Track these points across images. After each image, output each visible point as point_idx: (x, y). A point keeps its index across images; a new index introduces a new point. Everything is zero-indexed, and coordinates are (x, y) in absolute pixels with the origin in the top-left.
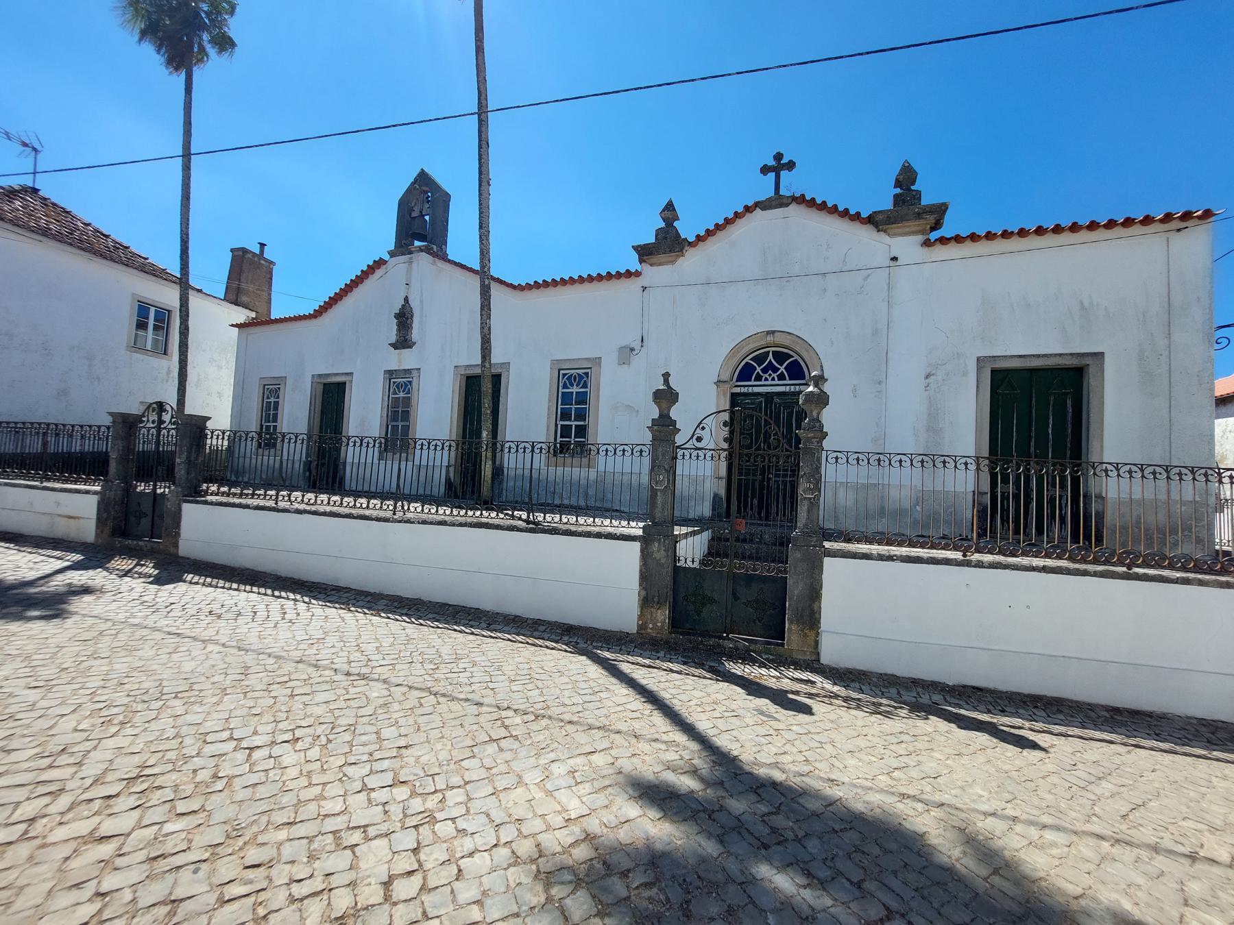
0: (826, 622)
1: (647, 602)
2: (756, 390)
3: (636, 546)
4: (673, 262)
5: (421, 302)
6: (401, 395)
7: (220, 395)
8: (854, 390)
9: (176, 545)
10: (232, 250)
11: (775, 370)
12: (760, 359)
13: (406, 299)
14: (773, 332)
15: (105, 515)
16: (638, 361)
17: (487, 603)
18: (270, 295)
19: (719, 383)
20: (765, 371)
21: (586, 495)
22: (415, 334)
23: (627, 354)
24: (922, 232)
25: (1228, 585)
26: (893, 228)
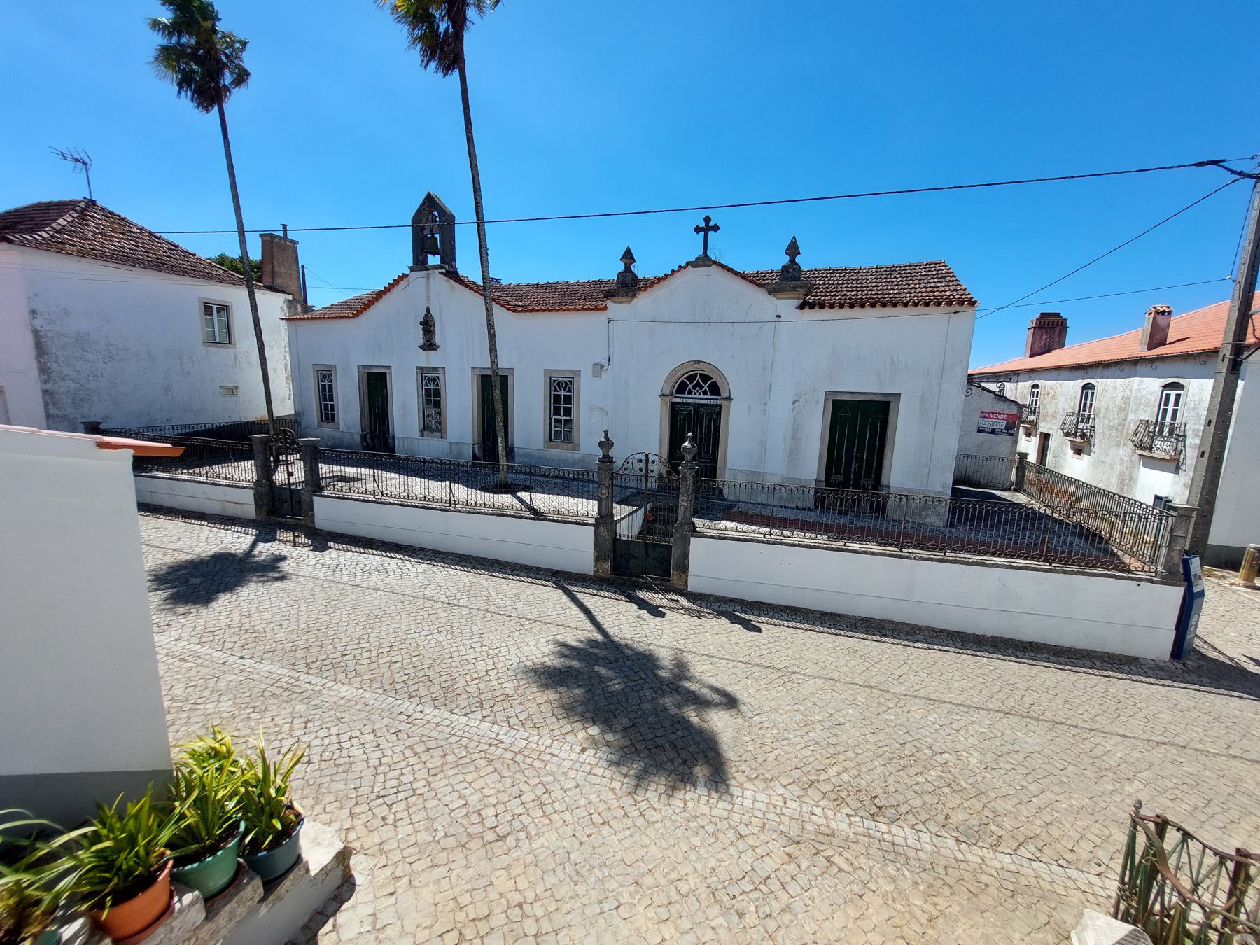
0: (691, 571)
4: (630, 302)
8: (749, 408)
9: (313, 522)
11: (701, 387)
12: (692, 378)
13: (428, 309)
14: (698, 362)
20: (694, 387)
22: (438, 339)
23: (599, 368)
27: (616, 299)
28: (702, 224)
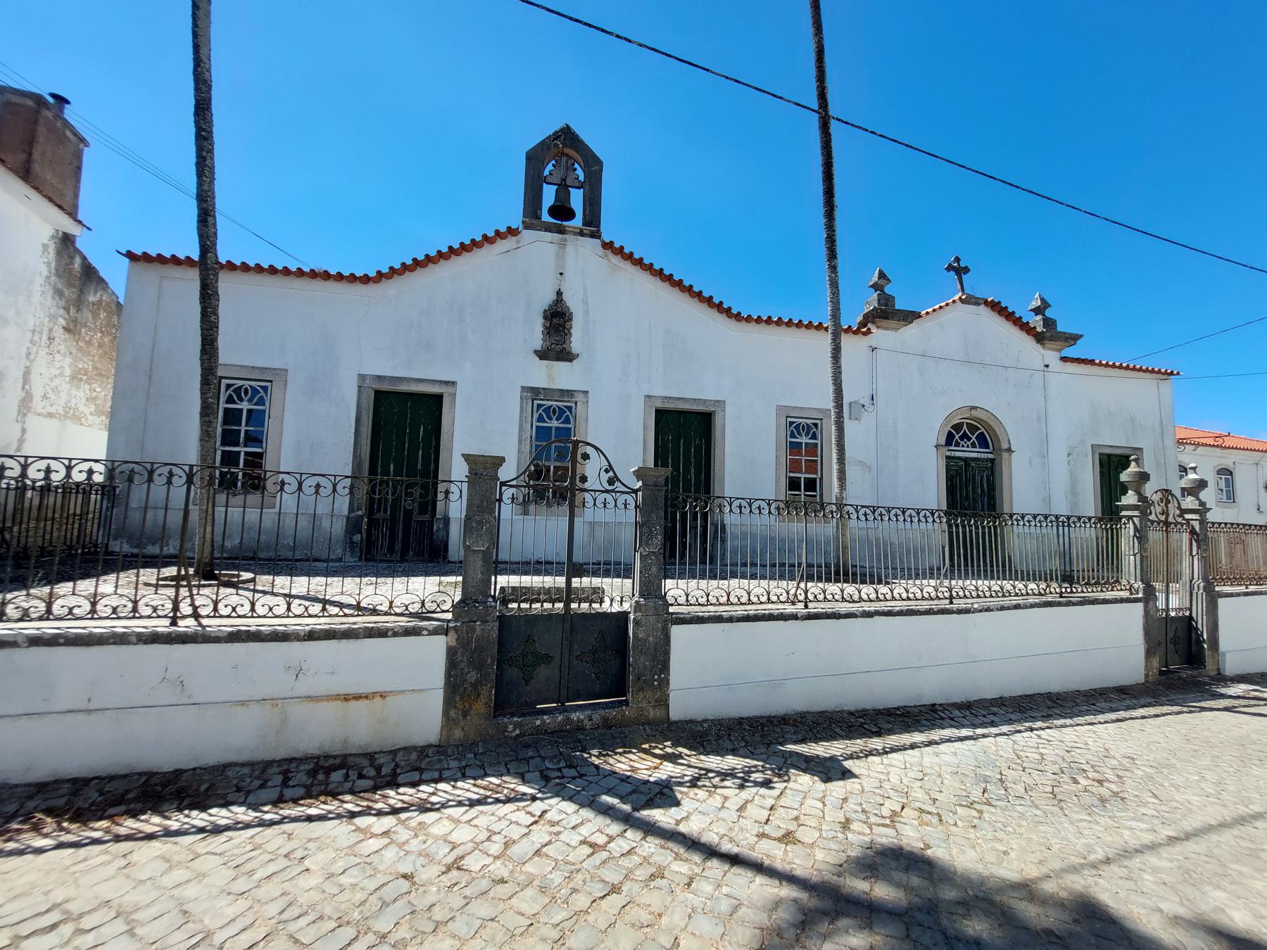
1: (1149, 653)
3: (1140, 606)
4: (897, 329)
5: (585, 302)
6: (555, 424)
9: (664, 703)
11: (969, 439)
12: (957, 427)
13: (559, 293)
14: (976, 408)
15: (473, 676)
18: (76, 195)
20: (962, 438)
27: (885, 323)
28: (962, 264)
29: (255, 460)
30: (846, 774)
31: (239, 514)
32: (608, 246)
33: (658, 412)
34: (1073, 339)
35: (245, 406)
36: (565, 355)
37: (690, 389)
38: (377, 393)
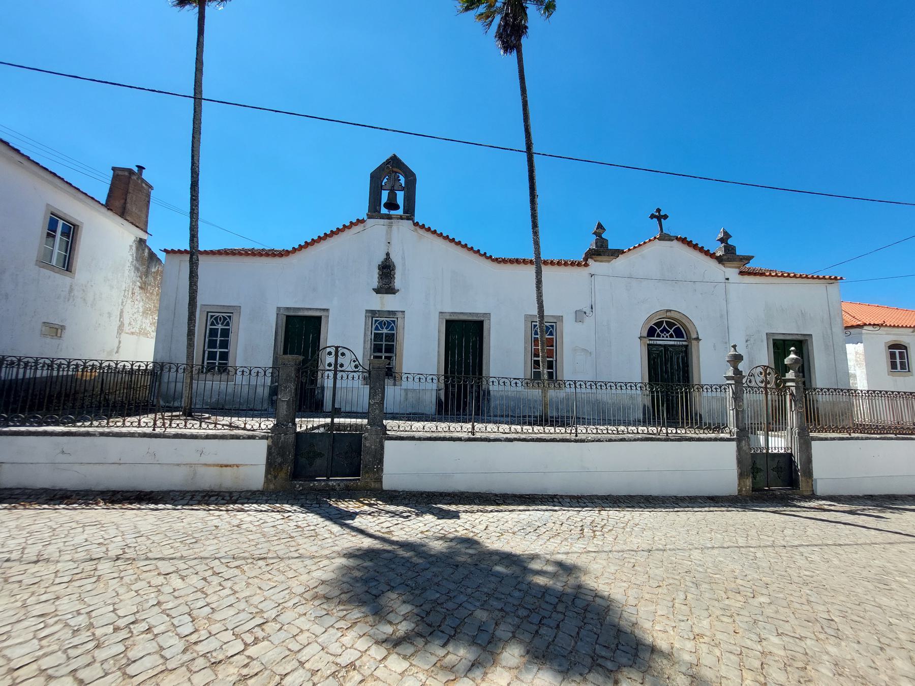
0: (816, 475)
1: (741, 476)
2: (659, 342)
3: (734, 444)
4: (609, 261)
5: (403, 258)
6: (385, 331)
7: (110, 314)
8: (714, 346)
9: (379, 480)
10: (114, 169)
11: (668, 332)
12: (659, 324)
13: (388, 254)
14: (670, 311)
15: (279, 460)
16: (589, 321)
17: (655, 490)
18: (147, 216)
19: (640, 338)
20: (662, 331)
21: (557, 409)
22: (398, 283)
23: (580, 316)
24: (739, 268)
25: (912, 439)
26: (728, 264)
27: (599, 258)
28: (662, 213)
29: (224, 356)
30: (458, 517)
31: (212, 385)
32: (416, 224)
33: (447, 321)
34: (748, 259)
35: (220, 327)
36: (391, 290)
37: (467, 306)
38: (288, 317)
